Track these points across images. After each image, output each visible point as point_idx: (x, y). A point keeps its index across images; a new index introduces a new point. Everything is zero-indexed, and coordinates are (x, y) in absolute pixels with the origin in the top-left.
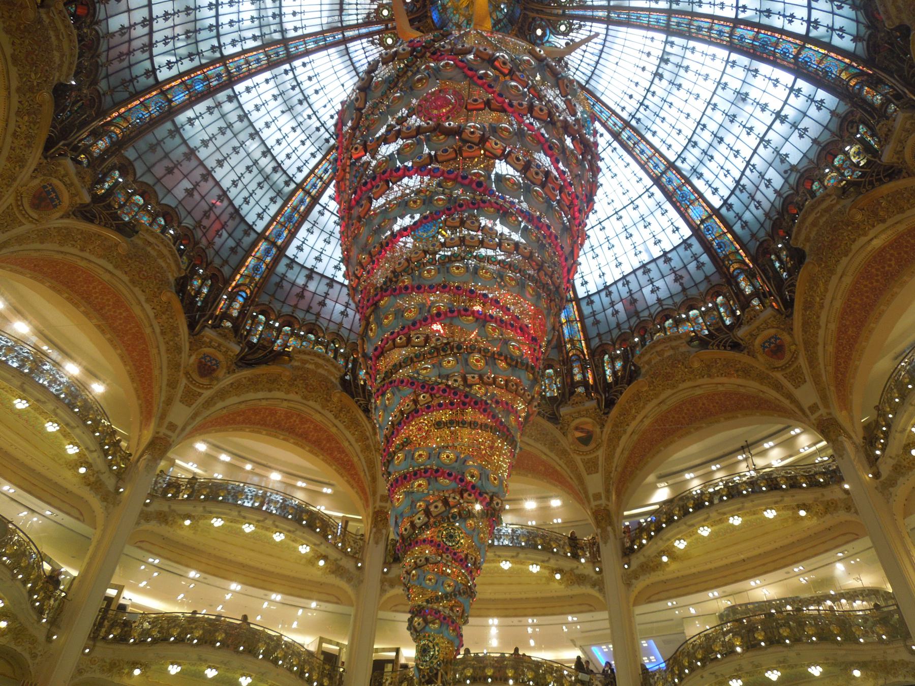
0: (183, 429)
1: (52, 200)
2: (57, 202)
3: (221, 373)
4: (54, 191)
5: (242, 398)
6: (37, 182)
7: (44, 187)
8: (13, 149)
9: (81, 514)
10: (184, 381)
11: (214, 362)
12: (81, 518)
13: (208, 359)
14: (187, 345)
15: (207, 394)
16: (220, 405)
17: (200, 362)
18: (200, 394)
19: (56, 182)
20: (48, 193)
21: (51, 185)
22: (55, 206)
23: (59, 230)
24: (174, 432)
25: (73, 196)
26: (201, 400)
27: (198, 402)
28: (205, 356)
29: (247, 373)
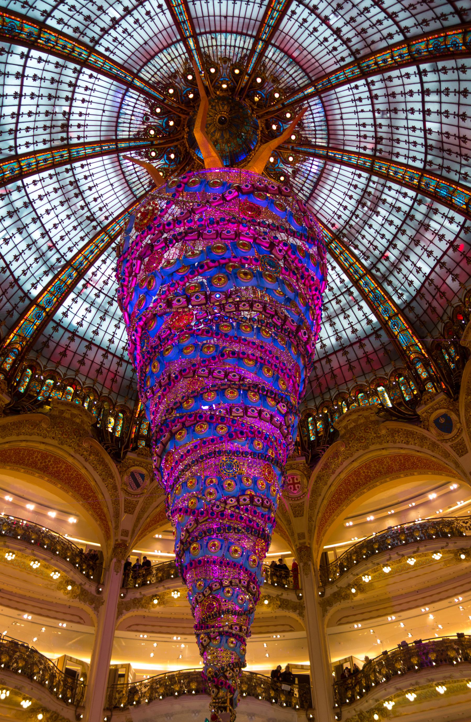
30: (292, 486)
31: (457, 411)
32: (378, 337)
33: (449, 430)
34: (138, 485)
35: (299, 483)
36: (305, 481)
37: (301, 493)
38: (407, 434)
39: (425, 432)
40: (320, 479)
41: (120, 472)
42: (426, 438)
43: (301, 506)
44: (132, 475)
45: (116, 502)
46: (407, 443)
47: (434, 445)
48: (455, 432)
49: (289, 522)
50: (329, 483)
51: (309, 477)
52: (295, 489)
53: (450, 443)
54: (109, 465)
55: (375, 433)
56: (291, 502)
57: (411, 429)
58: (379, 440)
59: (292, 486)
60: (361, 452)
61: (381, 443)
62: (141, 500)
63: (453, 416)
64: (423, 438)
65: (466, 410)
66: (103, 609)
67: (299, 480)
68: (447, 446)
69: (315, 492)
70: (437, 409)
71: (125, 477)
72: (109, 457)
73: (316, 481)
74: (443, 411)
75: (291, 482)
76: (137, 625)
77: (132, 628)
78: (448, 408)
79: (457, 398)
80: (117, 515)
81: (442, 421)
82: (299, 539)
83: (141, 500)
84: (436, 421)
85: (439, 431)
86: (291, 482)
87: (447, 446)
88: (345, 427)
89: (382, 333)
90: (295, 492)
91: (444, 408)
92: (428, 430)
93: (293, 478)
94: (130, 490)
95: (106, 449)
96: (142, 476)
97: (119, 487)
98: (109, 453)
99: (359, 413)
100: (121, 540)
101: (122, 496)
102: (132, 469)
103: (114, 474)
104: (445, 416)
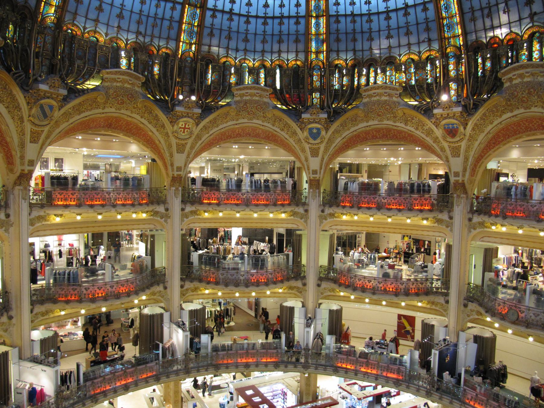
1: (453, 127)
2: (455, 126)
4: (448, 125)
6: (441, 130)
7: (445, 128)
8: (422, 133)
19: (444, 122)
20: (449, 127)
21: (445, 125)
22: (457, 128)
23: (473, 129)
25: (453, 117)
30: (182, 130)
31: (327, 130)
32: (297, 23)
33: (315, 139)
34: (45, 116)
35: (189, 128)
36: (194, 128)
37: (188, 137)
38: (285, 125)
39: (298, 131)
40: (206, 129)
41: (28, 103)
42: (297, 134)
43: (184, 146)
44: (42, 107)
45: (22, 133)
46: (283, 130)
47: (299, 140)
48: (318, 141)
49: (171, 155)
50: (211, 133)
51: (197, 125)
52: (184, 132)
53: (310, 145)
54: (17, 96)
55: (263, 113)
56: (177, 141)
57: (289, 123)
58: (263, 119)
59: (182, 130)
60: (245, 120)
61: (263, 122)
62: (46, 129)
63: (323, 133)
64: (295, 133)
65: (333, 132)
66: (11, 229)
67: (190, 126)
68: (307, 147)
69: (199, 137)
70: (316, 123)
71: (34, 111)
72: (18, 89)
73: (201, 129)
74: (318, 126)
75: (183, 126)
76: (38, 231)
77: (34, 234)
78: (323, 126)
79: (333, 121)
80: (22, 145)
81: (315, 131)
82: (177, 171)
83: (46, 129)
84: (311, 130)
85: (308, 135)
86: (183, 126)
87: (307, 147)
88: (242, 96)
89: (302, 21)
90: (183, 134)
91: (321, 124)
92: (301, 129)
93: (185, 124)
94: (37, 122)
95: (15, 80)
96: (51, 107)
97: (26, 118)
98: (18, 84)
99: (258, 91)
100: (28, 170)
101: (28, 127)
102: (42, 101)
103: (21, 105)
104: (318, 129)
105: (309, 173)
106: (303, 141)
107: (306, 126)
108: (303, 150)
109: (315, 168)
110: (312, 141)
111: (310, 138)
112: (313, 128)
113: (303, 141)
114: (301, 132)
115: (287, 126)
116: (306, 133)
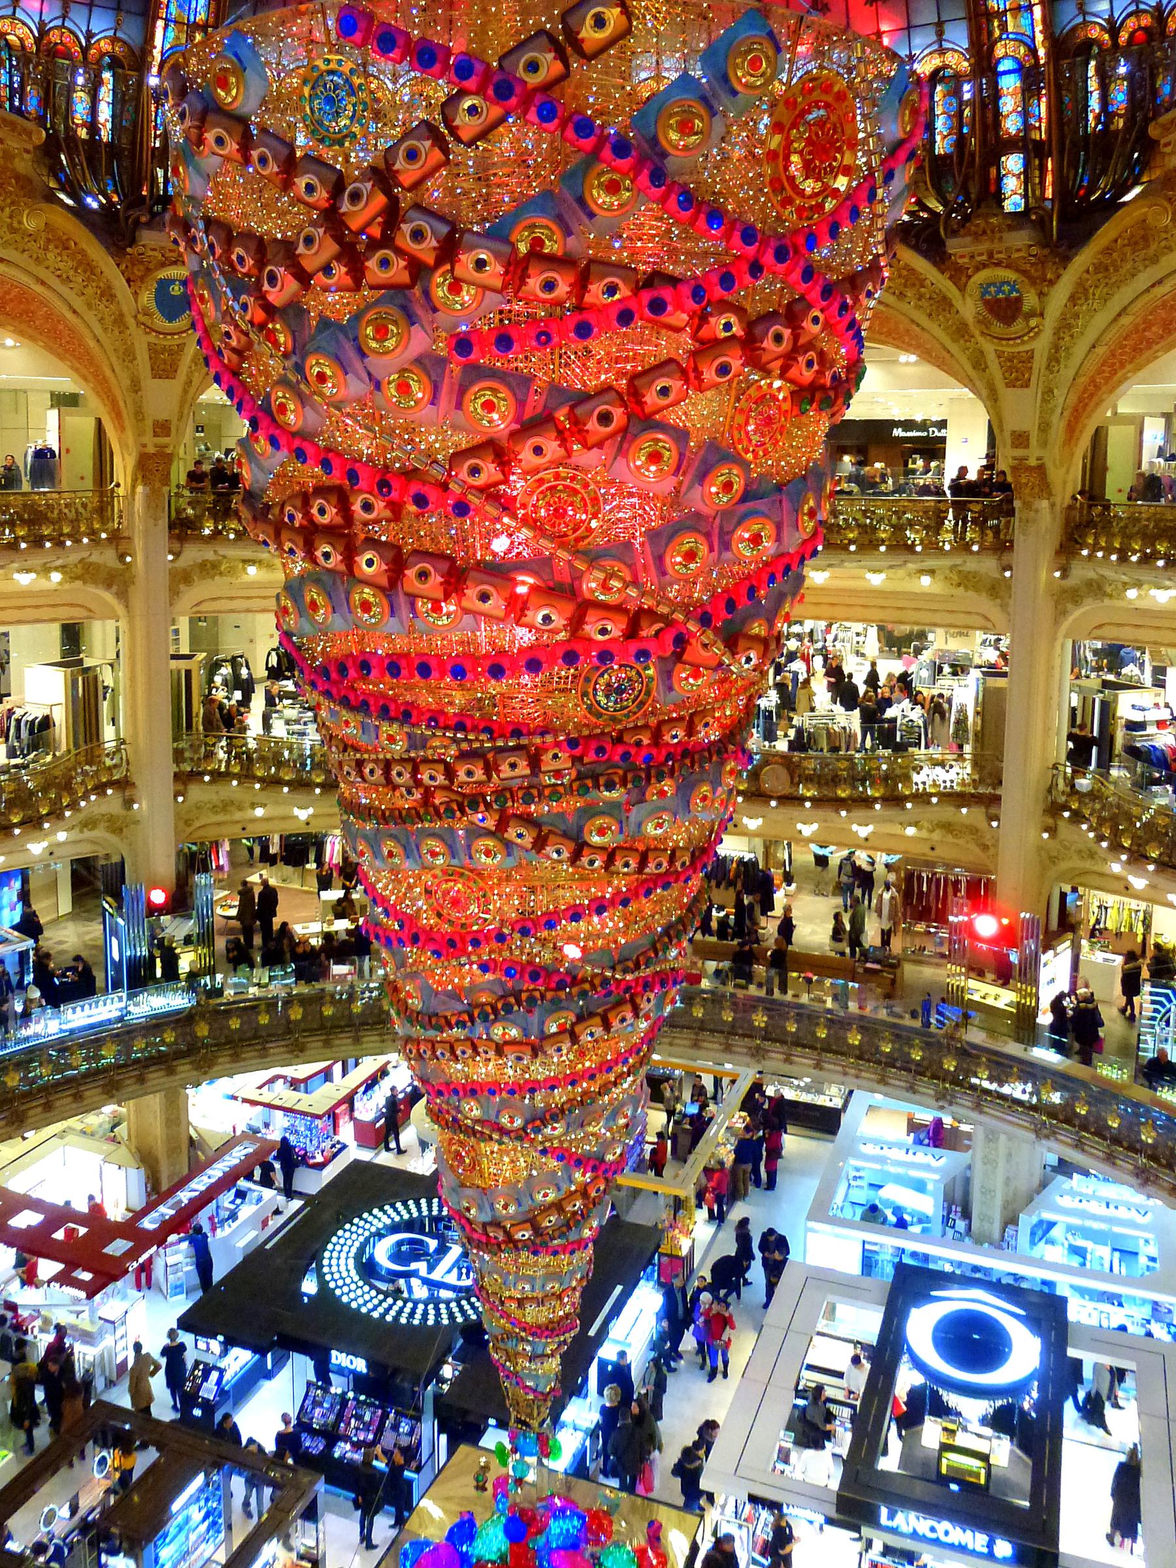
0: (1045, 427)
3: (1030, 300)
5: (1115, 305)
9: (987, 619)
10: (989, 348)
11: (1006, 288)
12: (989, 625)
13: (992, 289)
14: (949, 284)
15: (1041, 346)
16: (1080, 350)
17: (987, 303)
18: (1031, 355)
24: (1027, 446)
26: (1039, 362)
27: (1035, 372)
28: (984, 288)
29: (1084, 259)
53: (152, 338)
64: (107, 294)
81: (176, 290)
84: (164, 284)
87: (141, 342)
92: (128, 281)
105: (140, 433)
106: (131, 322)
107: (148, 270)
108: (129, 355)
109: (162, 417)
110: (160, 322)
111: (158, 315)
112: (172, 281)
113: (131, 322)
114: (129, 291)
115: (88, 267)
116: (147, 298)
